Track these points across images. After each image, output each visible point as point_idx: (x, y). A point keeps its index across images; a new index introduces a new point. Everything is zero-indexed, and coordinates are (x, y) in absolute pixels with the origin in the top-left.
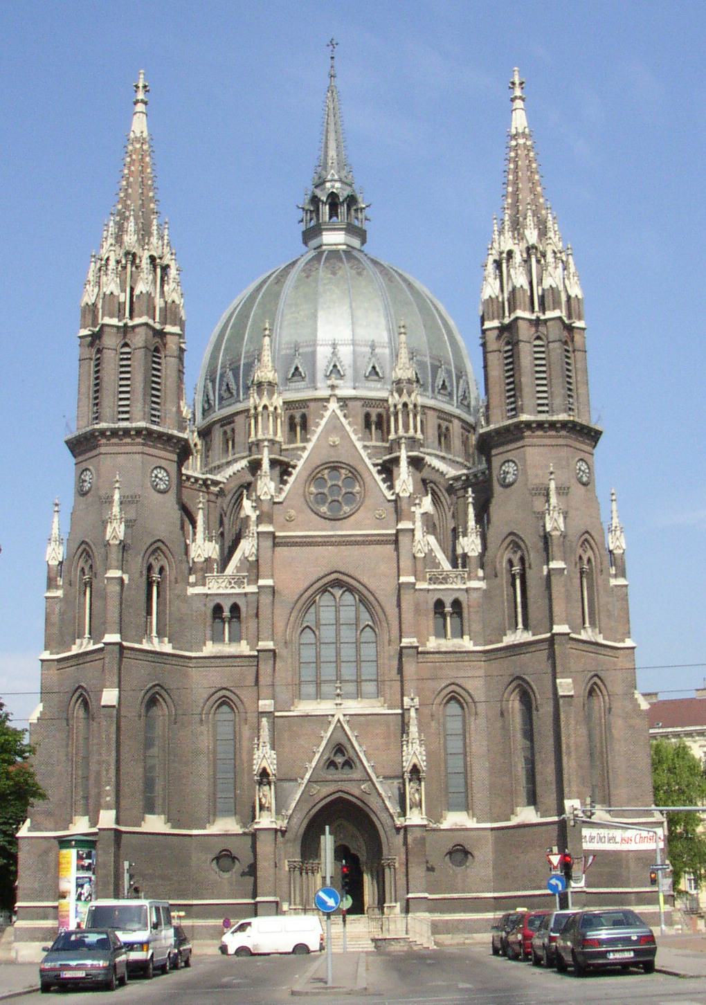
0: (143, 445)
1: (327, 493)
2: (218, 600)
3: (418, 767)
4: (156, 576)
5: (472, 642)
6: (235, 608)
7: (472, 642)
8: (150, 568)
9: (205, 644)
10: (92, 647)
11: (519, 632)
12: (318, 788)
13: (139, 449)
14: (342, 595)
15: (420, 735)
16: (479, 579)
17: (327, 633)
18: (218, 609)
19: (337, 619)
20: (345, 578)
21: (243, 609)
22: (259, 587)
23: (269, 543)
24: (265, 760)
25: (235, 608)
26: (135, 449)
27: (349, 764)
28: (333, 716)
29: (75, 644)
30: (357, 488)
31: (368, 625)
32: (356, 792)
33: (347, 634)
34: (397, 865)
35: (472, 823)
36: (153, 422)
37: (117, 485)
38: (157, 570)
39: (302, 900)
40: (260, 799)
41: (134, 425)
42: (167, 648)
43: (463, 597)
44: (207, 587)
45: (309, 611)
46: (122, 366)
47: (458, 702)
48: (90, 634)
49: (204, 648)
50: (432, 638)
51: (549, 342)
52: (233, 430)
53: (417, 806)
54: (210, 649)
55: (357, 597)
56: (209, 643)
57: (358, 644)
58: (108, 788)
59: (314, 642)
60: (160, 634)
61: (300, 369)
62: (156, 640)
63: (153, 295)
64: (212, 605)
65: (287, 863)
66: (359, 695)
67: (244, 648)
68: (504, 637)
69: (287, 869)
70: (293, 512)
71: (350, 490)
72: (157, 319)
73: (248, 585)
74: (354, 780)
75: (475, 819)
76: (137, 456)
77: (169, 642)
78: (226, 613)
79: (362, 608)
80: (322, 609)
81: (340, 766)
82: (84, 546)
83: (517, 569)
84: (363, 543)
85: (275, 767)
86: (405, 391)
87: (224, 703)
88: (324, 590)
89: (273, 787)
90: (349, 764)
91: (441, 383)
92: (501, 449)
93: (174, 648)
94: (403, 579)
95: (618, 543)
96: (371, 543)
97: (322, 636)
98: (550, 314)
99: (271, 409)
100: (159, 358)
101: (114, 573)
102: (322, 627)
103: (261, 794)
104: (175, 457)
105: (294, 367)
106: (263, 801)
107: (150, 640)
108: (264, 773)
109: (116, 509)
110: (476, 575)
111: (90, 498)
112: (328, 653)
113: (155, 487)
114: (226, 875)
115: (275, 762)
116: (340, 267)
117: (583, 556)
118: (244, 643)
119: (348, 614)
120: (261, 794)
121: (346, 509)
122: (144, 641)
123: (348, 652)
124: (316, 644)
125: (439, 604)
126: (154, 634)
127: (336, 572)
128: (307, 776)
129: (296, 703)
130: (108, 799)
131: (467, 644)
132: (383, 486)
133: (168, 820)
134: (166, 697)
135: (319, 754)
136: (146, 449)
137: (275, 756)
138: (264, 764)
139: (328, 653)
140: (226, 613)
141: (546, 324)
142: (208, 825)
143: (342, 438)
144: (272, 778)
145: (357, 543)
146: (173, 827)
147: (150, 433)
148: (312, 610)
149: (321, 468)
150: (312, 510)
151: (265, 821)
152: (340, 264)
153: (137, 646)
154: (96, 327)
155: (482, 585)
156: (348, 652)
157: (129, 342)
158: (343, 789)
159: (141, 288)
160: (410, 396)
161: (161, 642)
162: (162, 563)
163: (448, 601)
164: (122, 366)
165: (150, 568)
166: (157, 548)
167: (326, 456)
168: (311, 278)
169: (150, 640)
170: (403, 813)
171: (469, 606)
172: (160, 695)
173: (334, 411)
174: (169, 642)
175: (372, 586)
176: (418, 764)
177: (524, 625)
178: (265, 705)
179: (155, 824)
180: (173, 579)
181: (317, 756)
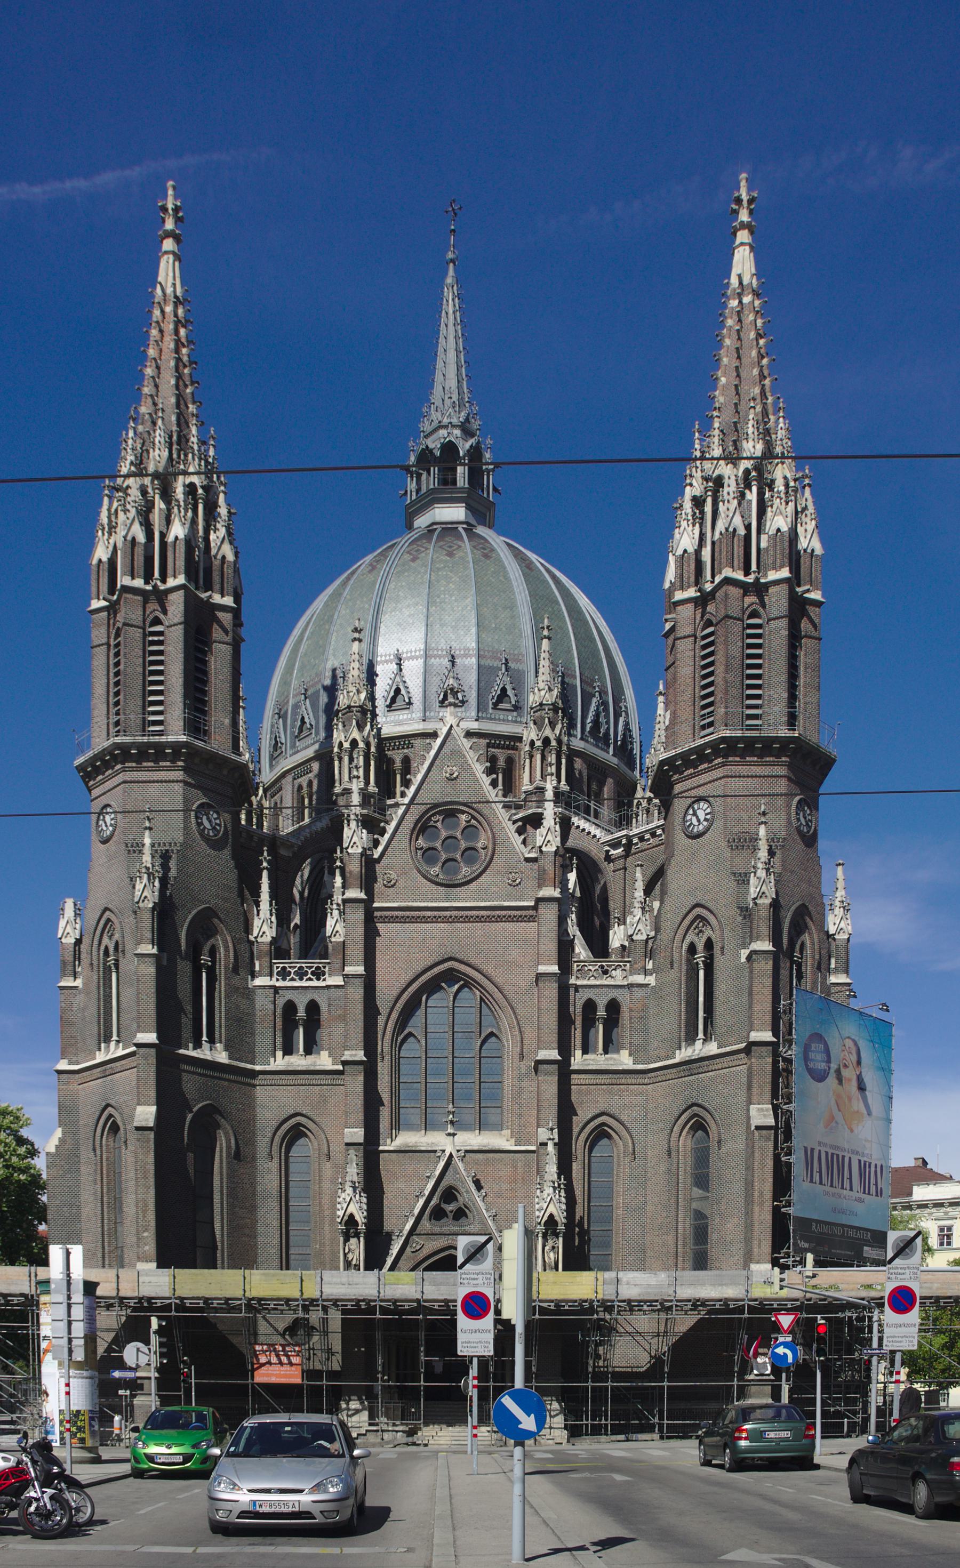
2: (289, 995)
20: (462, 968)
22: (346, 976)
28: (444, 1151)
40: (345, 1255)
44: (274, 979)
48: (118, 1036)
60: (212, 1041)
62: (206, 1046)
64: (281, 1002)
70: (394, 876)
73: (330, 975)
82: (108, 913)
83: (700, 957)
84: (489, 920)
88: (432, 987)
89: (362, 1239)
96: (499, 919)
116: (460, 547)
121: (465, 871)
144: (361, 1227)
145: (479, 919)
150: (419, 871)
152: (460, 543)
168: (418, 562)
175: (499, 980)
177: (705, 1033)
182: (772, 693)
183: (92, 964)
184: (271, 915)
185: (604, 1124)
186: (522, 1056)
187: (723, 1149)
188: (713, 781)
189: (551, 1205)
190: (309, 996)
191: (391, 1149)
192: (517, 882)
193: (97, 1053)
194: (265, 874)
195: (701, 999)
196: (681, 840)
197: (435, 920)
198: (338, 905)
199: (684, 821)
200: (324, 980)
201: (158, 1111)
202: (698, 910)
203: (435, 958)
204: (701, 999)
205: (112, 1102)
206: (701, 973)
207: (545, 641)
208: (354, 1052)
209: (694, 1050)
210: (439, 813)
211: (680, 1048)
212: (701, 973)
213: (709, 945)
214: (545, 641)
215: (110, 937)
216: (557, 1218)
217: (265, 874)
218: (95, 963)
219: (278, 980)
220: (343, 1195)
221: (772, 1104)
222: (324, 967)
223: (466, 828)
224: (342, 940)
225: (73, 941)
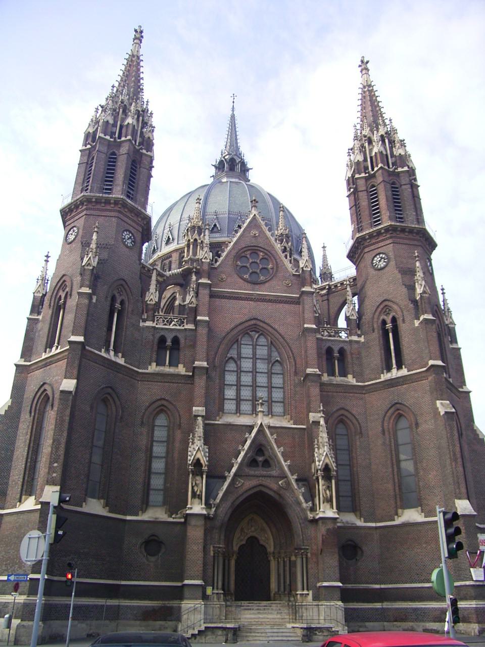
0: (119, 212)
1: (249, 267)
2: (162, 333)
3: (330, 466)
4: (118, 305)
5: (354, 379)
6: (176, 341)
7: (354, 379)
8: (113, 299)
9: (150, 365)
10: (59, 351)
11: (394, 371)
12: (243, 481)
14: (258, 337)
15: (329, 441)
16: (359, 336)
17: (247, 365)
18: (162, 340)
19: (254, 354)
20: (261, 324)
21: (182, 341)
23: (207, 292)
24: (199, 452)
25: (176, 341)
26: (112, 214)
27: (267, 464)
29: (45, 352)
30: (270, 266)
31: (277, 361)
32: (274, 486)
33: (262, 366)
34: (309, 555)
35: (360, 523)
36: (128, 197)
37: (96, 230)
38: (119, 301)
39: (223, 585)
40: (193, 487)
41: (114, 196)
42: (121, 361)
45: (233, 347)
46: (109, 165)
49: (149, 367)
50: (325, 375)
51: (401, 185)
52: (170, 262)
53: (328, 502)
54: (153, 368)
55: (269, 338)
57: (270, 374)
58: (56, 465)
59: (235, 369)
60: (116, 352)
61: (218, 226)
62: (112, 353)
63: (136, 127)
64: (158, 336)
65: (212, 548)
66: (270, 413)
67: (181, 370)
68: (382, 375)
69: (212, 553)
71: (266, 266)
72: (137, 144)
73: (187, 324)
74: (273, 477)
75: (362, 519)
76: (114, 219)
78: (169, 343)
79: (273, 349)
80: (242, 346)
81: (260, 464)
83: (389, 326)
85: (207, 459)
86: (284, 240)
87: (162, 411)
89: (204, 476)
90: (267, 464)
91: (300, 249)
92: (372, 247)
93: (125, 362)
94: (306, 326)
96: (281, 302)
97: (242, 366)
98: (400, 169)
99: (199, 241)
100: (136, 167)
101: (87, 290)
102: (242, 360)
103: (194, 484)
104: (141, 230)
105: (214, 224)
106: (196, 489)
107: (107, 351)
108: (197, 463)
109: (93, 246)
110: (356, 333)
111: (74, 245)
112: (246, 379)
113: (124, 243)
114: (153, 559)
115: (207, 454)
118: (181, 366)
119: (262, 352)
120: (194, 484)
122: (103, 350)
123: (262, 380)
124: (237, 371)
126: (112, 348)
127: (255, 319)
128: (234, 470)
130: (54, 475)
131: (351, 380)
132: (289, 266)
133: (106, 505)
134: (116, 399)
135: (245, 452)
136: (121, 216)
137: (207, 450)
138: (199, 456)
139: (246, 379)
140: (169, 343)
141: (399, 174)
142: (140, 512)
143: (260, 232)
144: (205, 468)
145: (270, 301)
146: (110, 512)
147: (125, 205)
148: (235, 346)
149: (245, 249)
151: (197, 508)
153: (96, 352)
154: (94, 143)
155: (362, 339)
156: (262, 380)
157: (116, 152)
158: (264, 483)
159: (129, 120)
160: (288, 244)
161: (116, 354)
162: (124, 298)
164: (109, 165)
165: (113, 299)
166: (122, 284)
167: (247, 242)
169: (107, 351)
170: (313, 509)
171: (352, 354)
172: (111, 396)
173: (255, 215)
176: (329, 463)
177: (397, 365)
178: (198, 410)
179: (95, 507)
180: (130, 309)
181: (242, 454)
182: (408, 212)
183: (50, 305)
184: (156, 291)
185: (342, 415)
186: (296, 373)
187: (420, 429)
188: (386, 245)
190: (174, 334)
192: (290, 285)
193: (44, 354)
195: (392, 347)
196: (372, 272)
197: (247, 299)
198: (193, 288)
199: (372, 263)
200: (183, 326)
201: (78, 383)
202: (386, 303)
203: (246, 318)
204: (392, 347)
205: (48, 382)
206: (391, 335)
207: (281, 212)
208: (201, 363)
209: (392, 374)
210: (249, 250)
211: (383, 373)
212: (391, 335)
213: (394, 320)
214: (281, 212)
215: (64, 291)
218: (52, 304)
219: (157, 324)
220: (192, 447)
222: (184, 319)
223: (262, 258)
224: (195, 306)
225: (41, 295)
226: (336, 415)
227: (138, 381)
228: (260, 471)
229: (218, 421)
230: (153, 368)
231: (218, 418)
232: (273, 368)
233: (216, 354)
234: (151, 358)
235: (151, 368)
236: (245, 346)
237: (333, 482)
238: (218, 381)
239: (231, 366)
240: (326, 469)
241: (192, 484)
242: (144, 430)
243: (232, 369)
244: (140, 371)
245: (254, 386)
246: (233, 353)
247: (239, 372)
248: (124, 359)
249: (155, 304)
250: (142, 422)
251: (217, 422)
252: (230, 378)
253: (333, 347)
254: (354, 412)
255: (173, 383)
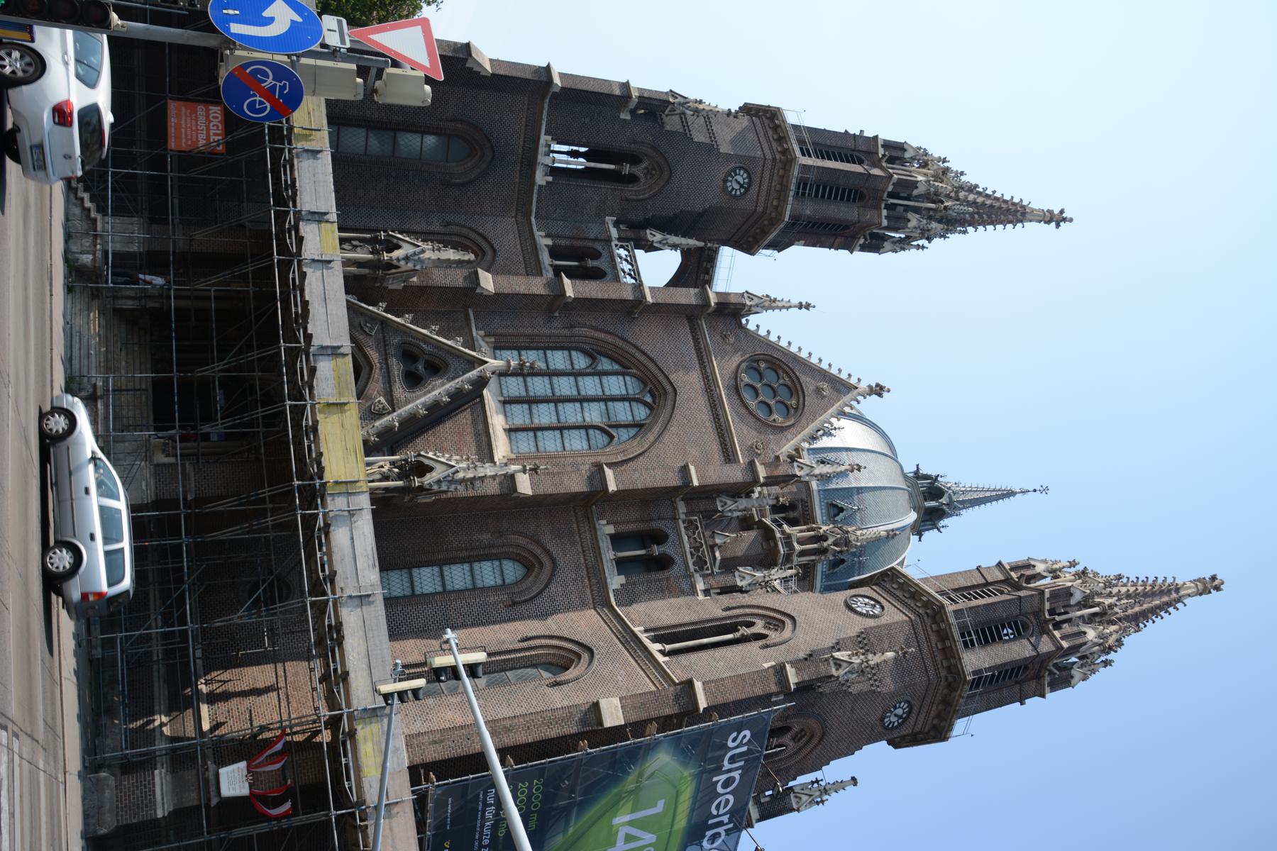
4: (627, 169)
9: (547, 236)
12: (373, 334)
13: (769, 156)
17: (590, 386)
43: (676, 570)
44: (617, 242)
47: (525, 577)
56: (549, 242)
64: (598, 246)
70: (732, 340)
76: (759, 153)
77: (547, 182)
95: (804, 798)
103: (355, 243)
112: (565, 386)
117: (789, 735)
119: (622, 412)
120: (355, 243)
123: (571, 413)
125: (660, 538)
129: (488, 339)
136: (769, 165)
139: (565, 386)
148: (616, 367)
156: (571, 413)
162: (643, 180)
163: (667, 549)
165: (635, 159)
174: (547, 182)
175: (666, 438)
189: (444, 468)
190: (608, 271)
191: (474, 334)
194: (701, 244)
216: (428, 475)
217: (701, 244)
221: (625, 725)
226: (538, 551)
227: (516, 218)
228: (397, 368)
229: (477, 334)
230: (544, 242)
231: (482, 333)
232: (598, 432)
233: (597, 329)
234: (559, 237)
235: (541, 236)
236: (623, 383)
237: (400, 483)
238: (547, 332)
239: (581, 362)
240: (423, 469)
241: (355, 239)
242: (436, 227)
243: (574, 362)
244: (533, 219)
245: (557, 400)
246: (605, 364)
247: (576, 374)
248: (544, 184)
249: (649, 241)
250: (449, 224)
251: (474, 330)
252: (558, 359)
253: (670, 540)
254: (553, 587)
255: (526, 268)
